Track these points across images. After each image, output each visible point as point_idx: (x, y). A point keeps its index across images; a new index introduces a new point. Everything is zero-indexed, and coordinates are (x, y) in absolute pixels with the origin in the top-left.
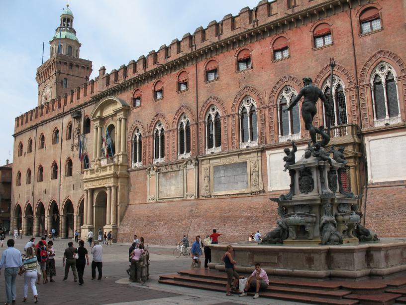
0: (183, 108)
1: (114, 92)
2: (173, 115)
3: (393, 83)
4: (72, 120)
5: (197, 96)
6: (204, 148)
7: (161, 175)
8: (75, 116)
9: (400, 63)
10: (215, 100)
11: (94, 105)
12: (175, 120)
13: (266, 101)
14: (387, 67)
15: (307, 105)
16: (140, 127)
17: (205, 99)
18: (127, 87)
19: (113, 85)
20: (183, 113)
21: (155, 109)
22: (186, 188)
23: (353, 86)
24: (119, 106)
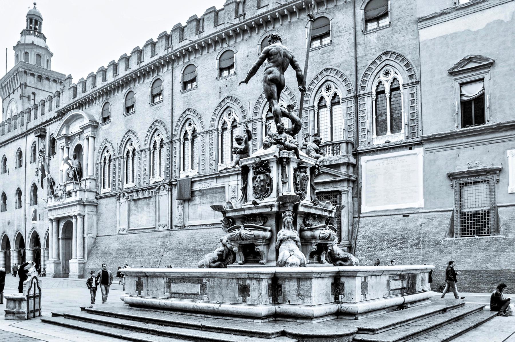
0: (156, 124)
1: (80, 105)
2: (145, 131)
3: (398, 92)
4: (36, 139)
5: (172, 108)
6: (178, 171)
7: (132, 203)
8: (39, 134)
9: (407, 67)
10: (192, 114)
11: (59, 122)
12: (147, 138)
13: (250, 115)
14: (392, 73)
15: (270, 73)
16: (109, 147)
17: (181, 112)
18: (96, 99)
19: (80, 96)
20: (157, 129)
21: (126, 125)
22: (157, 218)
23: (352, 95)
24: (86, 121)
